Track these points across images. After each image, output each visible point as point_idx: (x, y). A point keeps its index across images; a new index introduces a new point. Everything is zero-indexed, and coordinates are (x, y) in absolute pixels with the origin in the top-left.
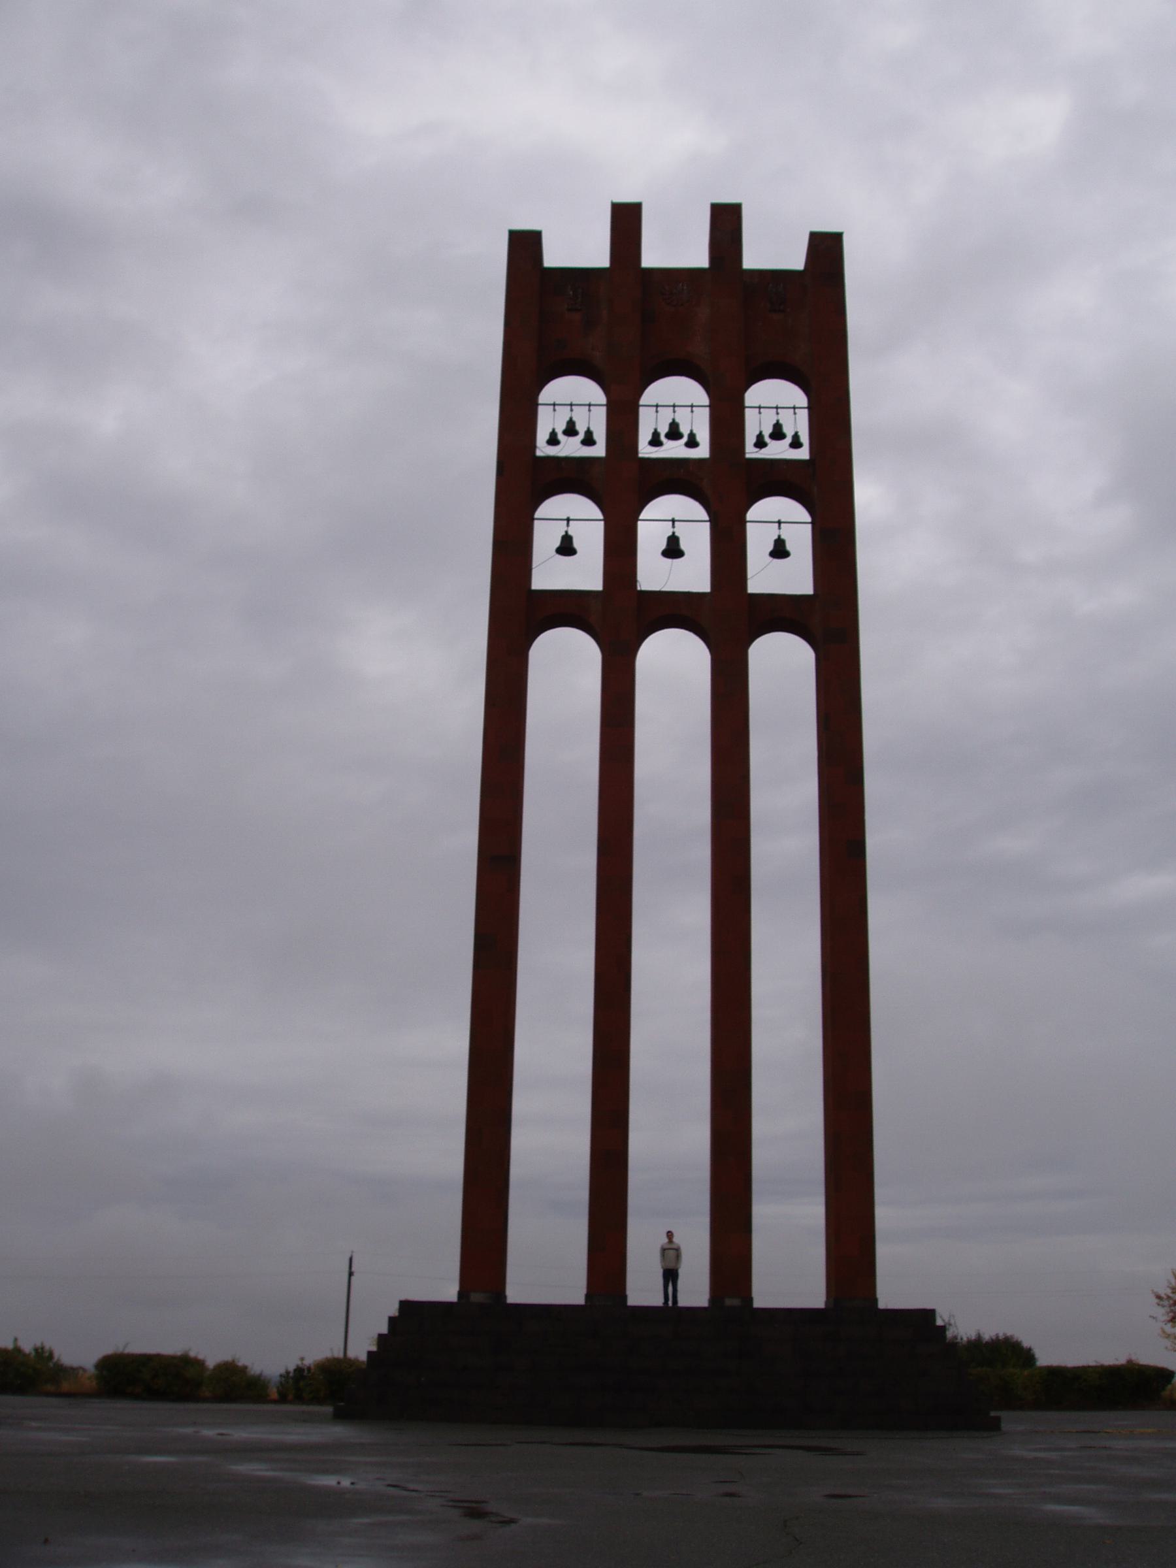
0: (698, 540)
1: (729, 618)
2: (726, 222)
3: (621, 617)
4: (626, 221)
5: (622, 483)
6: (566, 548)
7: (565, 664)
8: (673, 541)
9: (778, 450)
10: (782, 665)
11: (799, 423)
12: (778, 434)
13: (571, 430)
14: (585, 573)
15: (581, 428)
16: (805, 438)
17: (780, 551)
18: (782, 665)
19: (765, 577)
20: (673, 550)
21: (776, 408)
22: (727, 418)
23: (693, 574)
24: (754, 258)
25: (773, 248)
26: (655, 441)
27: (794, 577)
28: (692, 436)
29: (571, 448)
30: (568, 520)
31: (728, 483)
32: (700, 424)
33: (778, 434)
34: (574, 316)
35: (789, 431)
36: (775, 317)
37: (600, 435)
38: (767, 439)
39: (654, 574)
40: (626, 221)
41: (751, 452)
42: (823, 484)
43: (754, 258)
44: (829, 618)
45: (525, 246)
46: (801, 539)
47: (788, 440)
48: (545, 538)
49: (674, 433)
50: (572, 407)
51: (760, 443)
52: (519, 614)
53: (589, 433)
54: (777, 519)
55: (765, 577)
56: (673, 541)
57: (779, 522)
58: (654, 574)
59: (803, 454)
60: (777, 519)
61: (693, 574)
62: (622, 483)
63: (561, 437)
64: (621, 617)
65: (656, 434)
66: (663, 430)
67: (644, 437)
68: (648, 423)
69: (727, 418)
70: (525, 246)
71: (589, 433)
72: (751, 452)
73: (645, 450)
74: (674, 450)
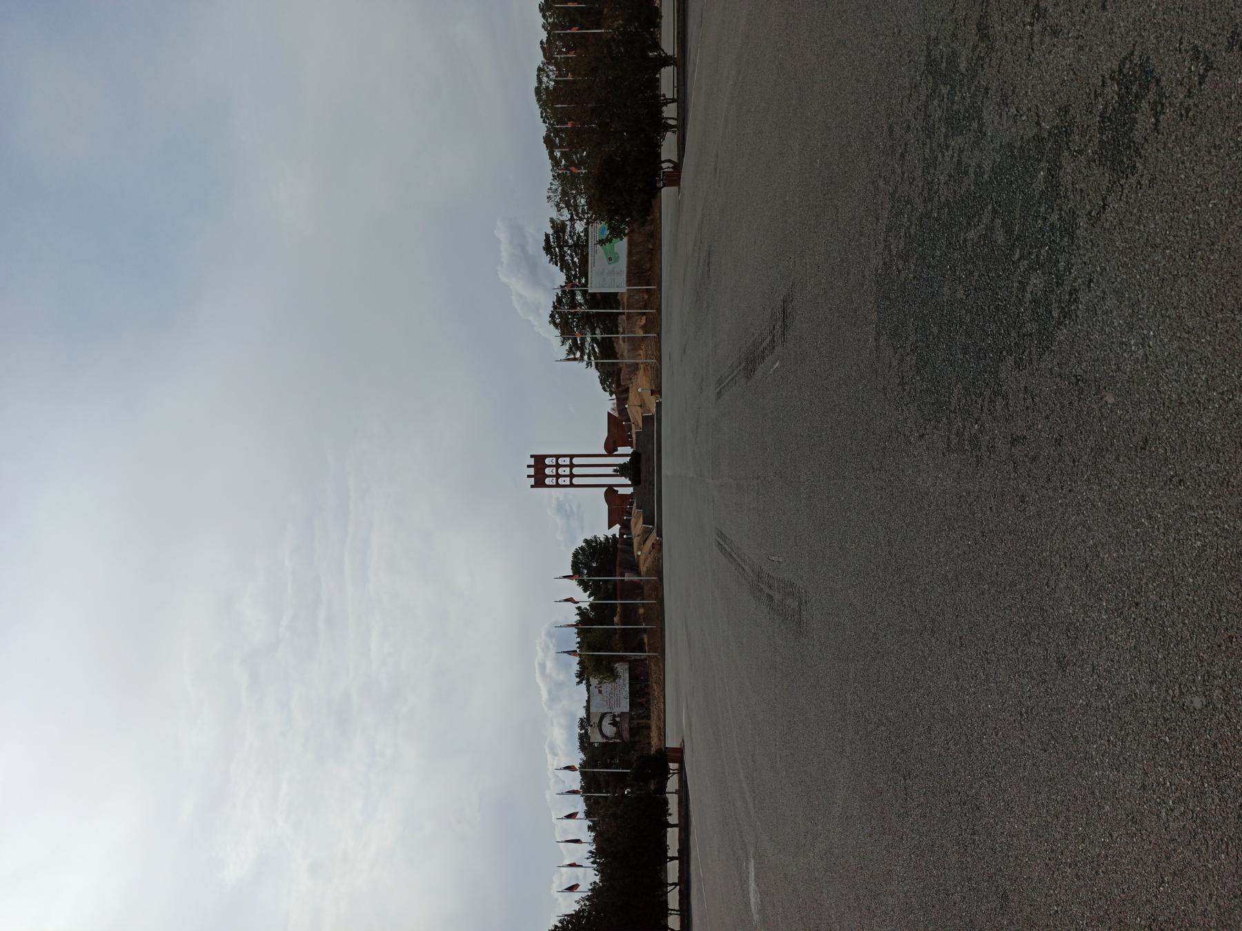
1: (572, 466)
2: (529, 466)
3: (572, 476)
4: (529, 476)
5: (558, 476)
7: (576, 481)
10: (576, 461)
18: (576, 461)
21: (548, 461)
23: (568, 470)
24: (532, 463)
25: (532, 462)
31: (558, 466)
34: (539, 481)
36: (539, 461)
39: (568, 472)
40: (529, 476)
42: (558, 457)
43: (532, 463)
44: (572, 457)
50: (548, 481)
52: (572, 485)
54: (561, 461)
58: (568, 472)
60: (561, 461)
61: (568, 470)
62: (558, 476)
64: (572, 476)
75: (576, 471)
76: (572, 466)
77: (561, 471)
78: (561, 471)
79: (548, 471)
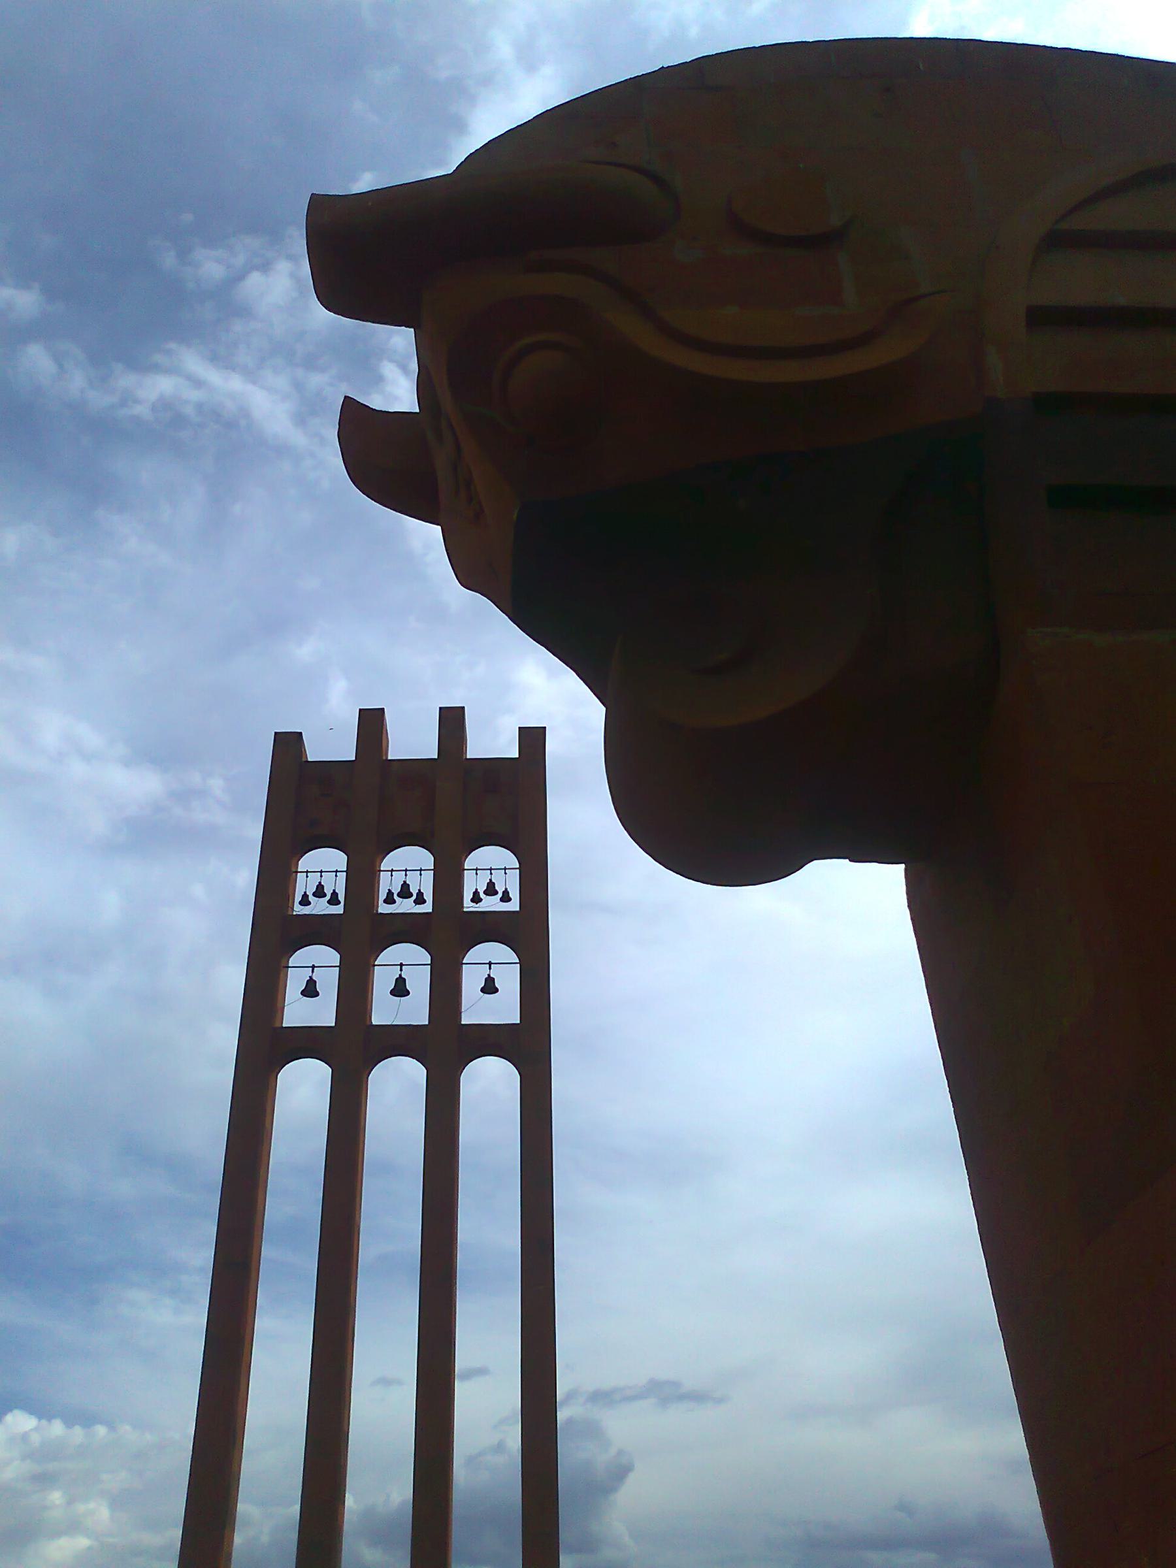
0: (420, 982)
1: (446, 1046)
2: (452, 722)
4: (372, 723)
5: (360, 933)
6: (310, 990)
8: (401, 981)
9: (491, 904)
11: (512, 883)
12: (491, 890)
13: (320, 892)
14: (321, 1013)
15: (328, 892)
16: (515, 894)
17: (490, 987)
19: (477, 1010)
20: (400, 989)
21: (490, 869)
22: (448, 878)
23: (415, 1010)
24: (478, 747)
25: (491, 740)
26: (390, 900)
27: (505, 1008)
28: (420, 894)
29: (320, 907)
30: (313, 967)
31: (449, 932)
32: (425, 884)
33: (491, 890)
35: (500, 889)
37: (341, 898)
38: (482, 895)
39: (385, 1011)
40: (372, 723)
41: (468, 905)
42: (527, 932)
43: (478, 747)
44: (527, 1045)
45: (288, 745)
46: (509, 980)
47: (500, 895)
48: (295, 982)
49: (405, 892)
51: (476, 899)
52: (265, 1046)
53: (334, 894)
54: (491, 963)
55: (477, 1010)
56: (401, 981)
57: (490, 964)
58: (385, 1011)
59: (514, 906)
60: (491, 963)
61: (415, 1010)
63: (311, 898)
64: (353, 1048)
65: (390, 893)
66: (396, 890)
67: (383, 895)
68: (387, 883)
69: (448, 878)
70: (288, 745)
71: (334, 894)
72: (468, 905)
73: (384, 908)
74: (406, 906)
75: (397, 1089)
76: (446, 1046)
77: (406, 961)
78: (406, 961)
79: (408, 868)
